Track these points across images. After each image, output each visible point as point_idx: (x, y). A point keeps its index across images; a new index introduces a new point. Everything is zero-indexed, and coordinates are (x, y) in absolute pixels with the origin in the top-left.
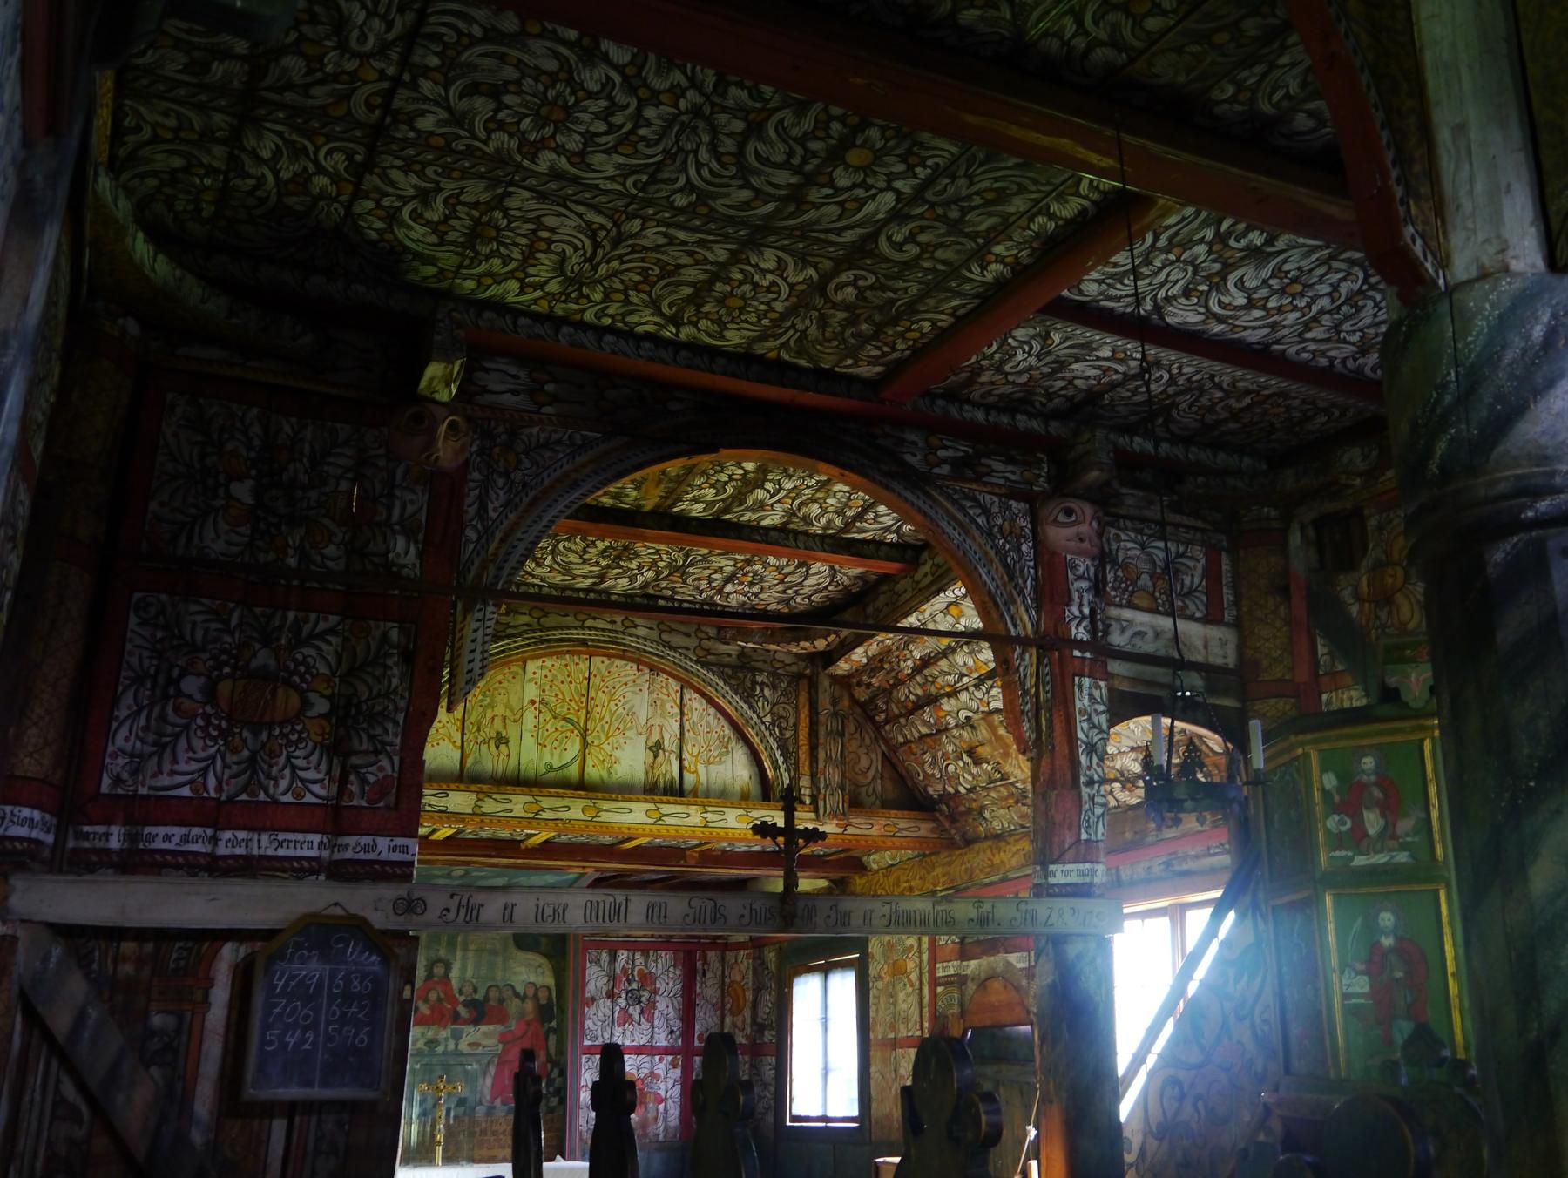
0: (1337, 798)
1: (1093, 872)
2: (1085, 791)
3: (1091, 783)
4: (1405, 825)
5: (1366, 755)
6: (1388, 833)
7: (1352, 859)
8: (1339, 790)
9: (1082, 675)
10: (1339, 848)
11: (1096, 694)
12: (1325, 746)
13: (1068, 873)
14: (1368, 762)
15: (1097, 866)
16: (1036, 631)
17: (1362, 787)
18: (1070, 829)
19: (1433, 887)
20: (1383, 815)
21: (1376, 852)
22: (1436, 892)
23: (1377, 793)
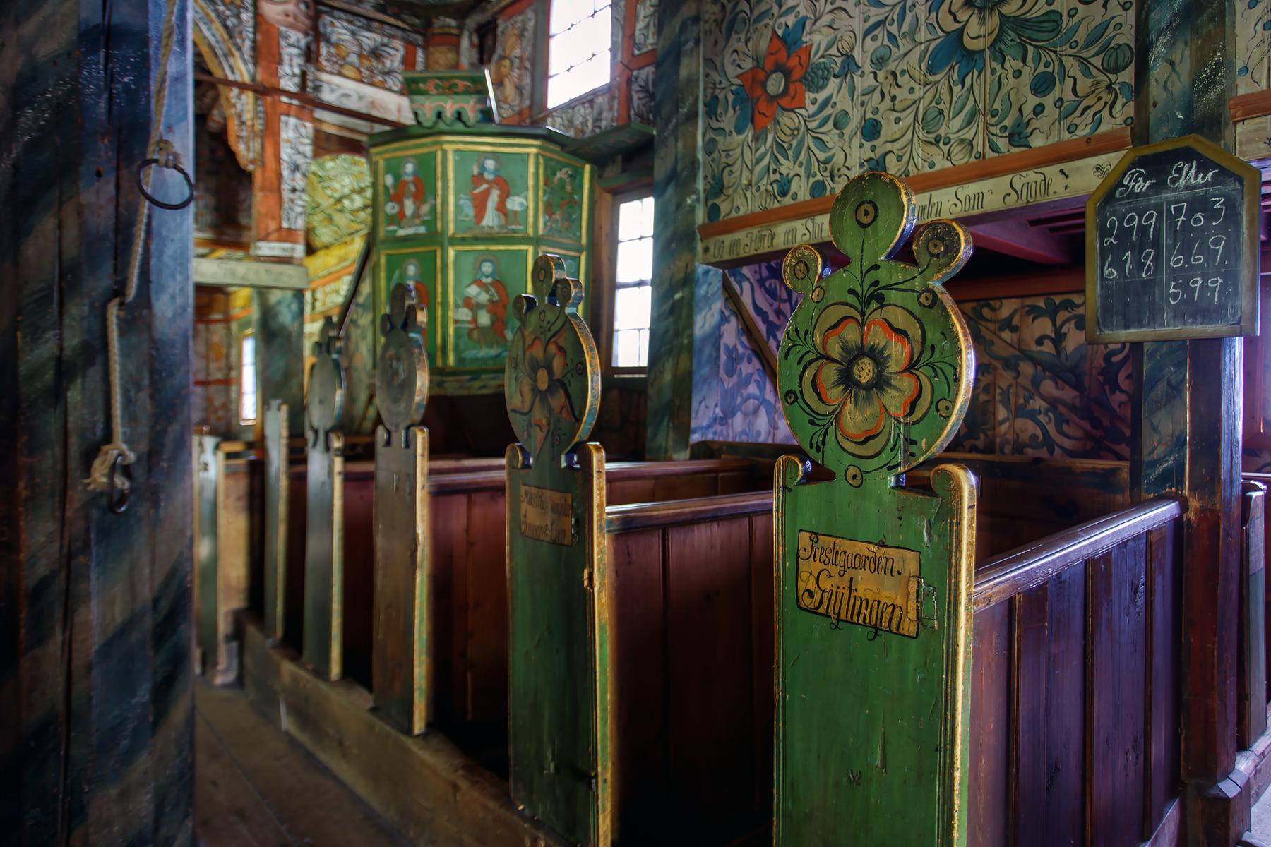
0: (392, 191)
1: (293, 250)
2: (286, 195)
3: (294, 190)
4: (425, 208)
5: (409, 162)
6: (416, 215)
7: (396, 231)
8: (395, 186)
9: (288, 115)
10: (391, 224)
11: (303, 131)
12: (387, 156)
13: (273, 249)
14: (409, 168)
15: (295, 246)
16: (253, 79)
17: (406, 183)
18: (273, 218)
19: (432, 248)
20: (415, 203)
21: (410, 226)
22: (435, 251)
23: (412, 188)
